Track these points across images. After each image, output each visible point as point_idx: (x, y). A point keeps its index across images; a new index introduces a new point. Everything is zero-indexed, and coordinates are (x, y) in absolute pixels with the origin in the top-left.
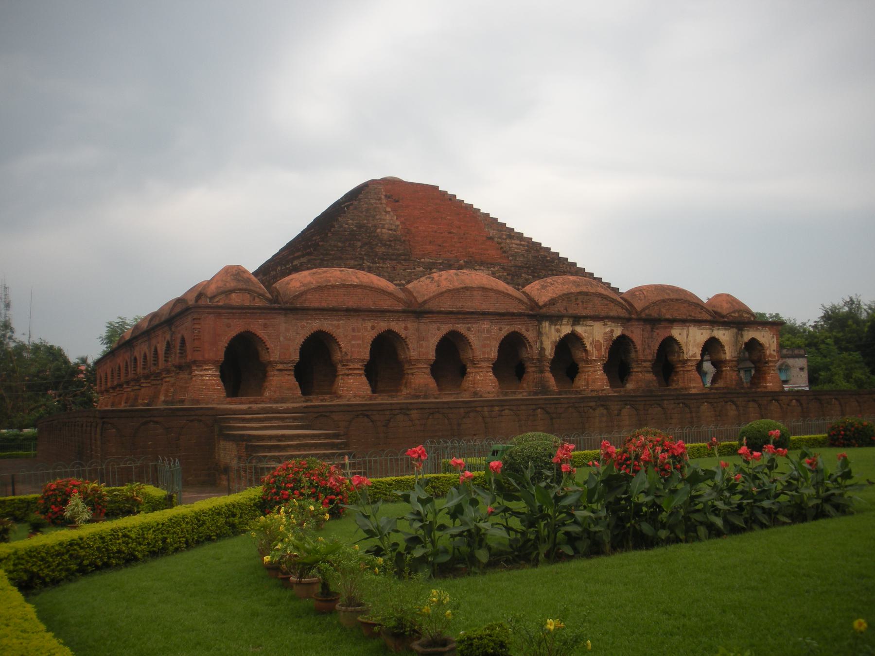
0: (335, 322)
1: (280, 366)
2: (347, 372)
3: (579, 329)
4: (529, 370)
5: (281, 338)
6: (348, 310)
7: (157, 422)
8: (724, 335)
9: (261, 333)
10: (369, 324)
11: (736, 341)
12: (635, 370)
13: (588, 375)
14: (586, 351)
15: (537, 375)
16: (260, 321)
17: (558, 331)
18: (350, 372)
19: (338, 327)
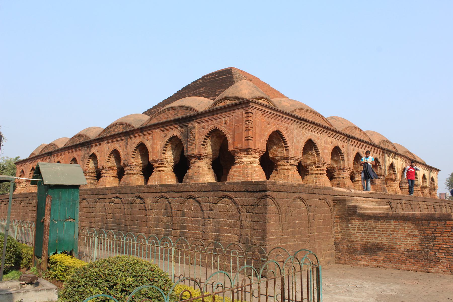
0: (317, 134)
1: (292, 162)
2: (320, 172)
3: (395, 161)
4: (377, 182)
5: (295, 140)
6: (324, 127)
7: (302, 199)
8: (426, 173)
9: (285, 134)
10: (330, 139)
11: (430, 177)
12: (404, 187)
13: (395, 188)
14: (395, 174)
15: (382, 186)
16: (285, 125)
17: (389, 160)
18: (322, 172)
19: (318, 139)
